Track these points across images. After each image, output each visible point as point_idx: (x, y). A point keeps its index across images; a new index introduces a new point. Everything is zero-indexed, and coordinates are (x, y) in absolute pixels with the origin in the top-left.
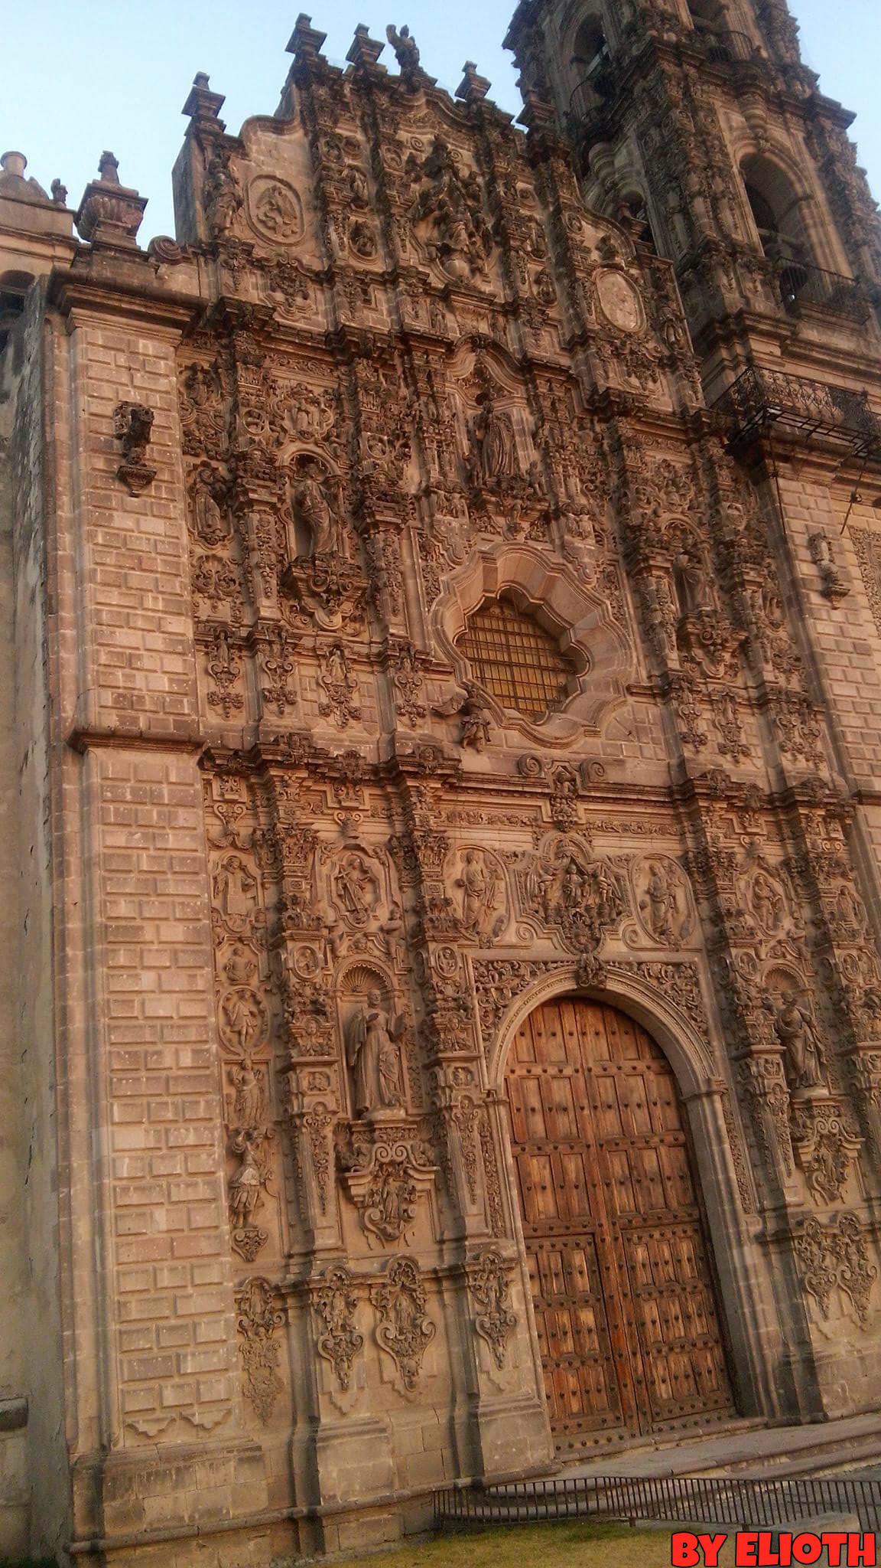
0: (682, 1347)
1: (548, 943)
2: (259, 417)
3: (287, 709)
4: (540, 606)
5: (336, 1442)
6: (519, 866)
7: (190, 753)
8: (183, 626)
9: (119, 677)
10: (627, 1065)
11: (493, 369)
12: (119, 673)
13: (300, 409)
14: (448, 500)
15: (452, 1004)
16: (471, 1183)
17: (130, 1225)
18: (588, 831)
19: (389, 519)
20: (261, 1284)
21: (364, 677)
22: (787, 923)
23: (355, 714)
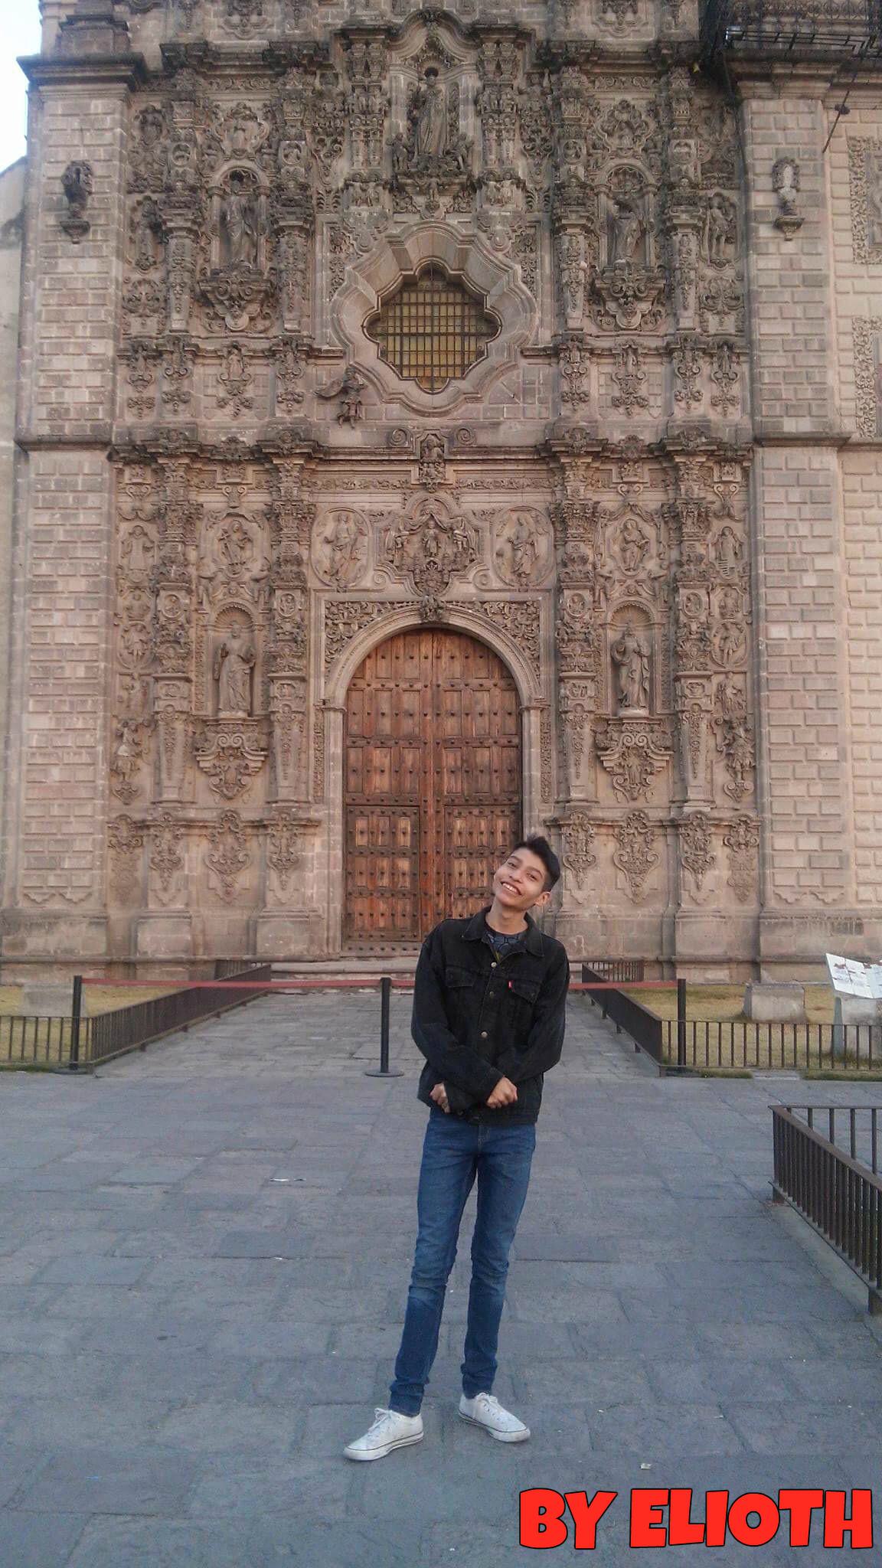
0: (482, 894)
1: (400, 587)
2: (186, 149)
3: (182, 407)
4: (459, 276)
5: (151, 920)
6: (381, 525)
7: (101, 450)
8: (105, 348)
9: (53, 396)
10: (475, 682)
11: (447, 40)
12: (53, 392)
13: (236, 129)
14: (364, 190)
15: (287, 638)
16: (285, 765)
17: (36, 776)
18: (456, 490)
19: (291, 223)
21: (260, 370)
22: (652, 565)
23: (248, 404)
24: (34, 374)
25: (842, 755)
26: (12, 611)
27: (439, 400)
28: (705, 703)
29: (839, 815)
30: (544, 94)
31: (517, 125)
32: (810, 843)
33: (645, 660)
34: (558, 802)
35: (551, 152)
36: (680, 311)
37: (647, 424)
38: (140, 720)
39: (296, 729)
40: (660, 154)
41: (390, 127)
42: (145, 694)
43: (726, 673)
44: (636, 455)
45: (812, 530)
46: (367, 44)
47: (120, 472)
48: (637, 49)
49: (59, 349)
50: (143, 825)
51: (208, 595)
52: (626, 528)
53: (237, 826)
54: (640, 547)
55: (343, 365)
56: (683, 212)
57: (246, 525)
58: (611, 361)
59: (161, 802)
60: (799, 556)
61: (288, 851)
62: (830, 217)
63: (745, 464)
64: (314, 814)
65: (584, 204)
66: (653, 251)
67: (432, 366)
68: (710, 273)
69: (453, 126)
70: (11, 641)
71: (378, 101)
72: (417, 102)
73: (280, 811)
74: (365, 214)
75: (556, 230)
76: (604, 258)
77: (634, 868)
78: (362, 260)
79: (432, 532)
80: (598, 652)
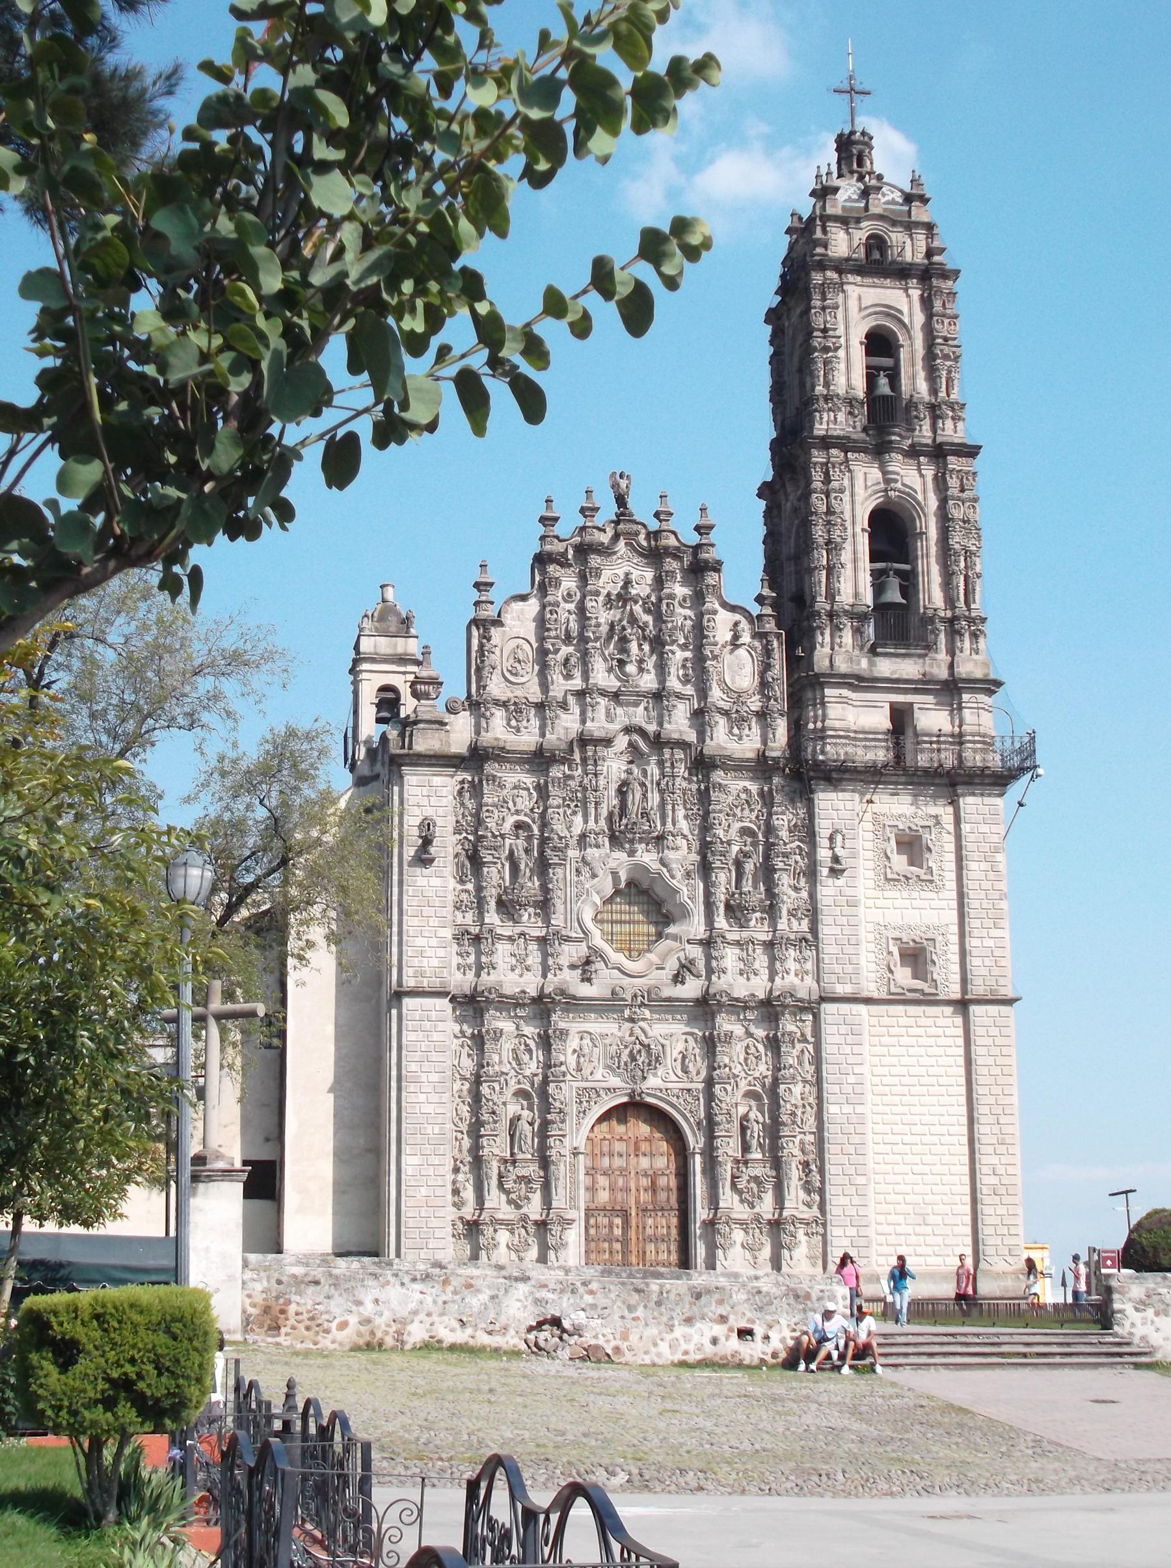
8: (448, 933)
11: (642, 744)
20: (461, 1218)
25: (869, 1180)
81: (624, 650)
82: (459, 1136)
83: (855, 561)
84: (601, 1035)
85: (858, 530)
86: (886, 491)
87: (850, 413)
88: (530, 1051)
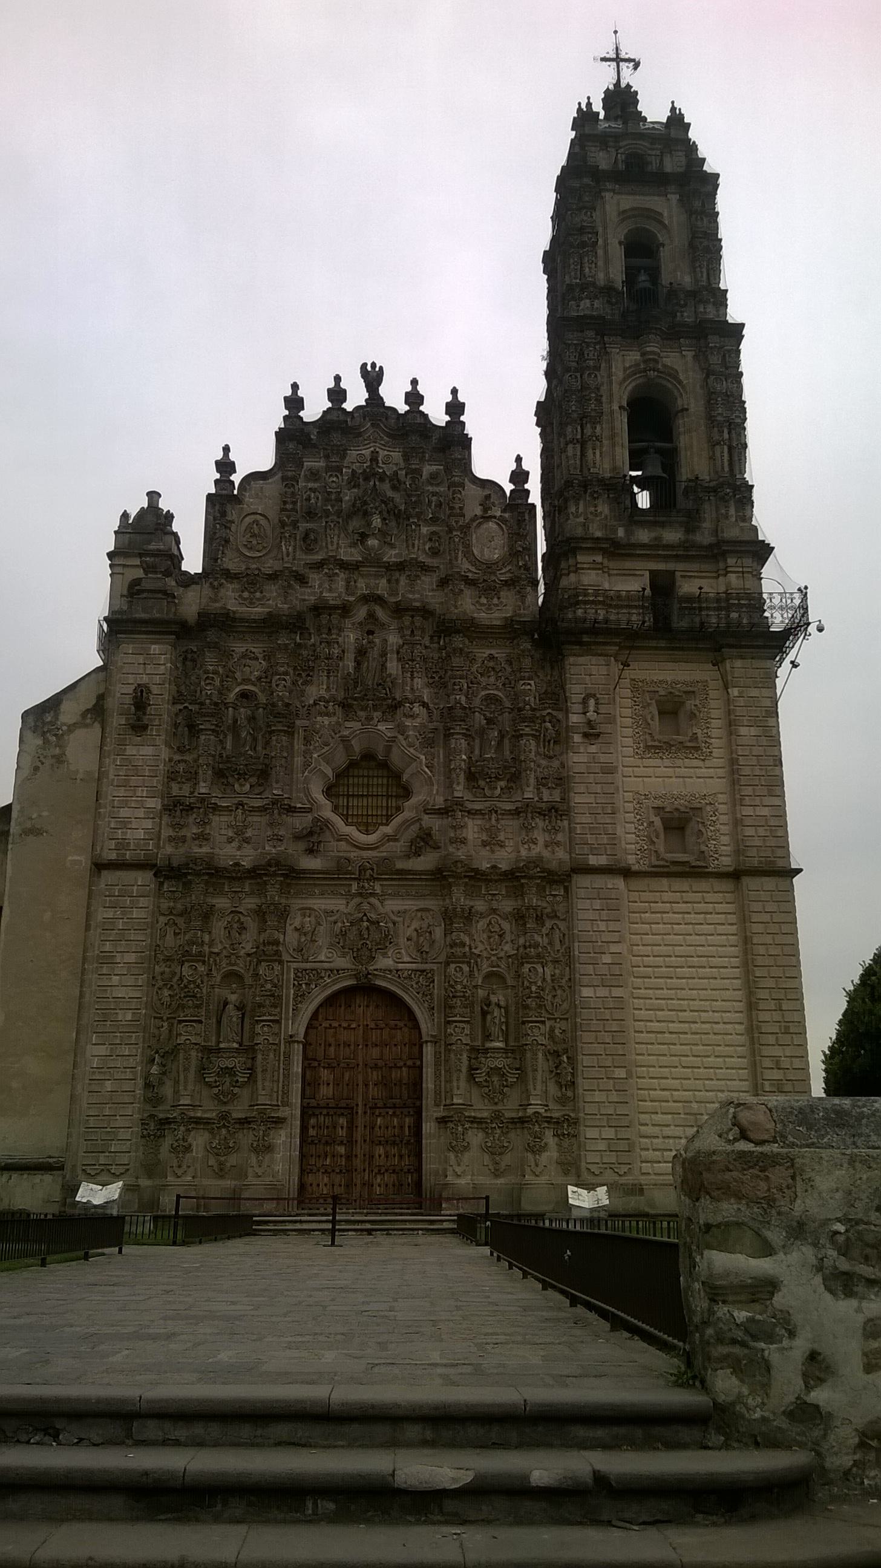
7: (151, 870)
8: (155, 804)
9: (119, 834)
11: (380, 613)
12: (120, 831)
13: (245, 666)
14: (326, 707)
21: (255, 819)
22: (507, 948)
23: (247, 841)
24: (106, 820)
25: (630, 1075)
26: (83, 974)
27: (372, 838)
28: (541, 1040)
29: (627, 1115)
30: (440, 649)
31: (424, 668)
32: (609, 1133)
33: (503, 1010)
34: (445, 1105)
35: (444, 685)
36: (525, 787)
37: (504, 858)
38: (167, 1049)
39: (272, 1055)
40: (513, 688)
41: (343, 666)
42: (170, 1031)
43: (555, 1019)
44: (496, 878)
45: (607, 927)
46: (330, 615)
47: (161, 884)
48: (498, 623)
49: (125, 804)
50: (167, 1121)
51: (216, 965)
52: (490, 923)
53: (229, 1122)
54: (501, 936)
55: (310, 817)
56: (526, 726)
57: (243, 919)
58: (481, 817)
59: (179, 1105)
60: (600, 944)
61: (263, 1140)
62: (619, 728)
63: (566, 884)
64: (279, 1114)
65: (464, 721)
66: (508, 748)
67: (368, 815)
68: (544, 762)
69: (383, 666)
70: (82, 995)
71: (336, 651)
72: (361, 653)
73: (262, 1112)
74: (326, 723)
75: (448, 736)
76: (477, 752)
77: (494, 1151)
78: (324, 751)
79: (365, 924)
80: (472, 1004)
81: (369, 524)
82: (159, 1023)
83: (612, 437)
84: (326, 912)
85: (616, 407)
86: (645, 371)
87: (608, 302)
88: (245, 928)
